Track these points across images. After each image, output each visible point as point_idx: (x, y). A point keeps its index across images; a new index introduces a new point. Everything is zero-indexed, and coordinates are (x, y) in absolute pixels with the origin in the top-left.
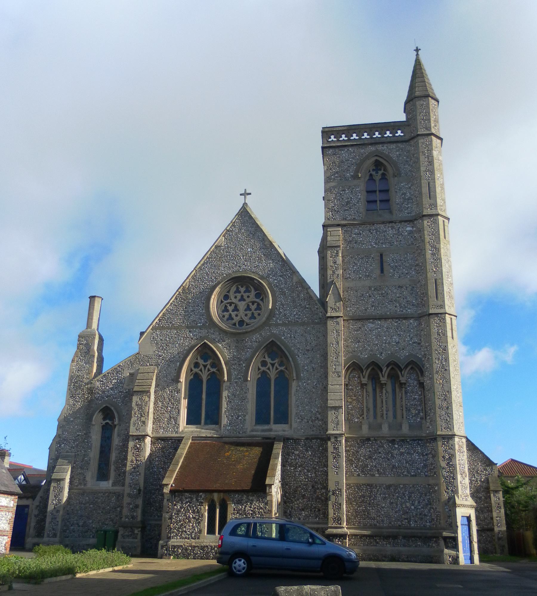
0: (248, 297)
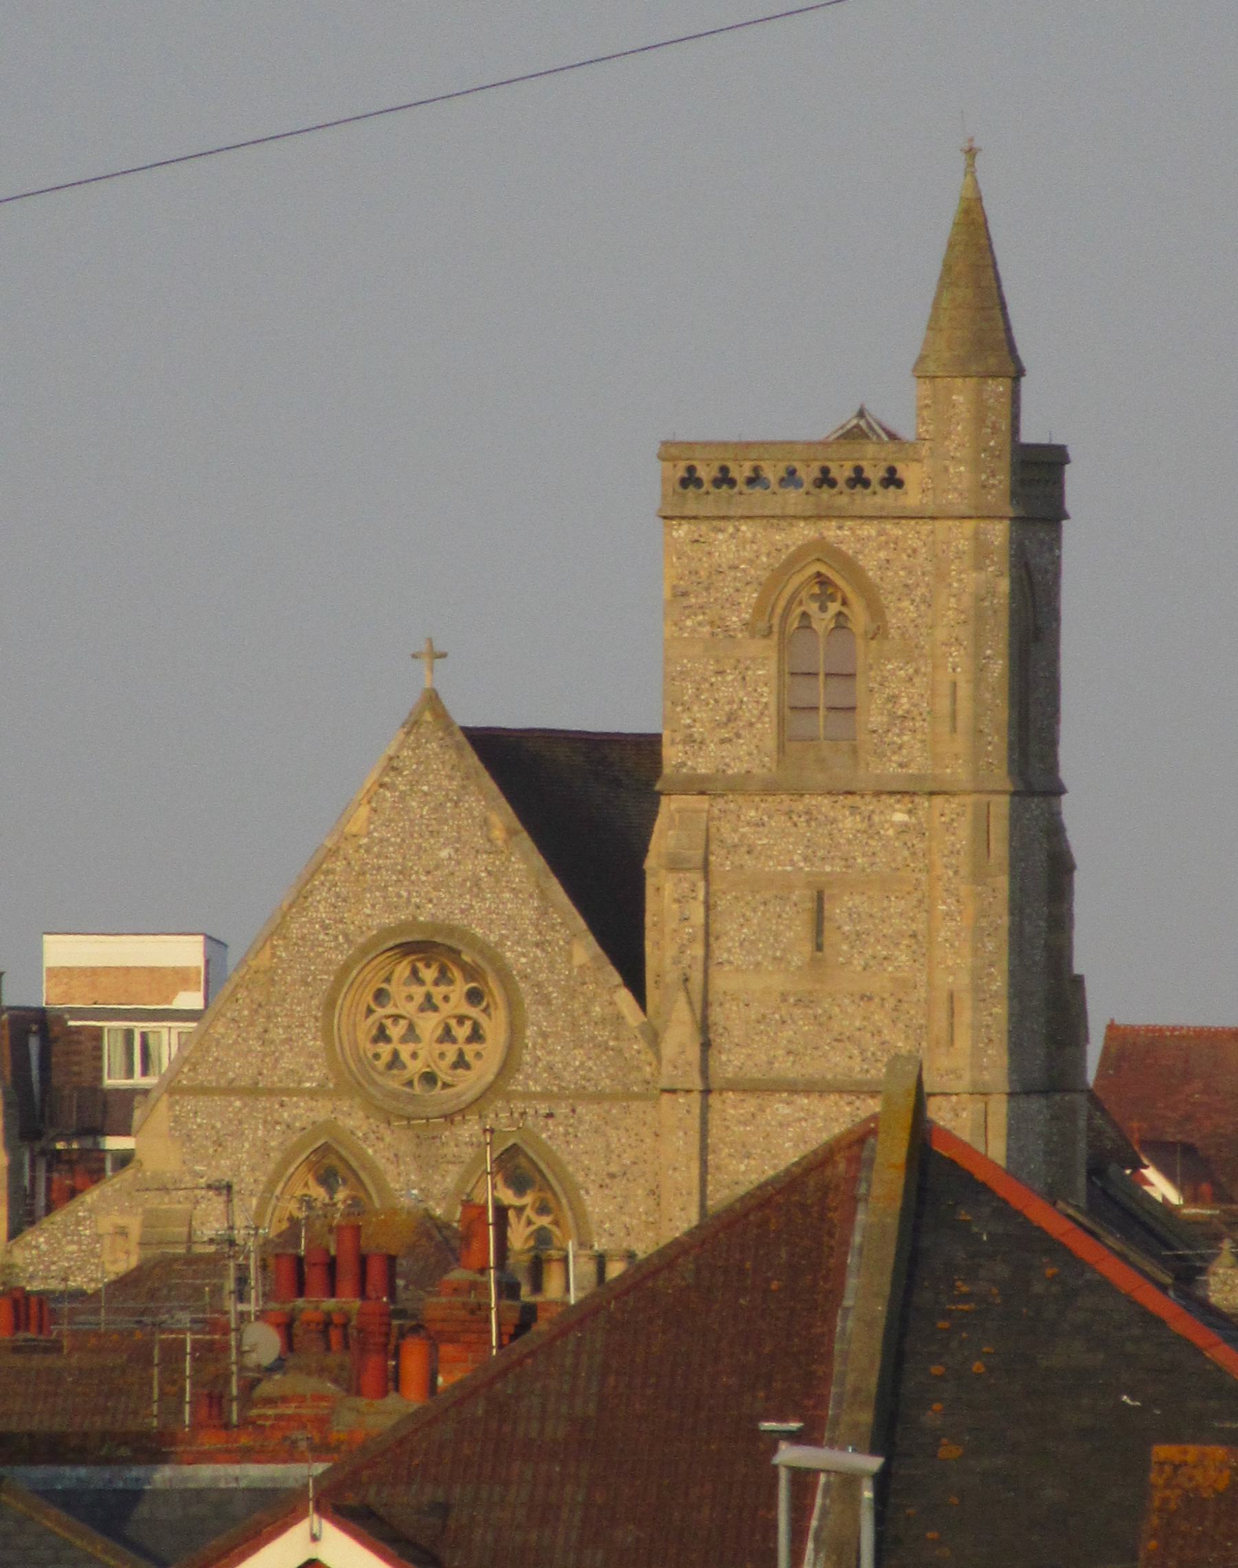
0: (446, 999)
